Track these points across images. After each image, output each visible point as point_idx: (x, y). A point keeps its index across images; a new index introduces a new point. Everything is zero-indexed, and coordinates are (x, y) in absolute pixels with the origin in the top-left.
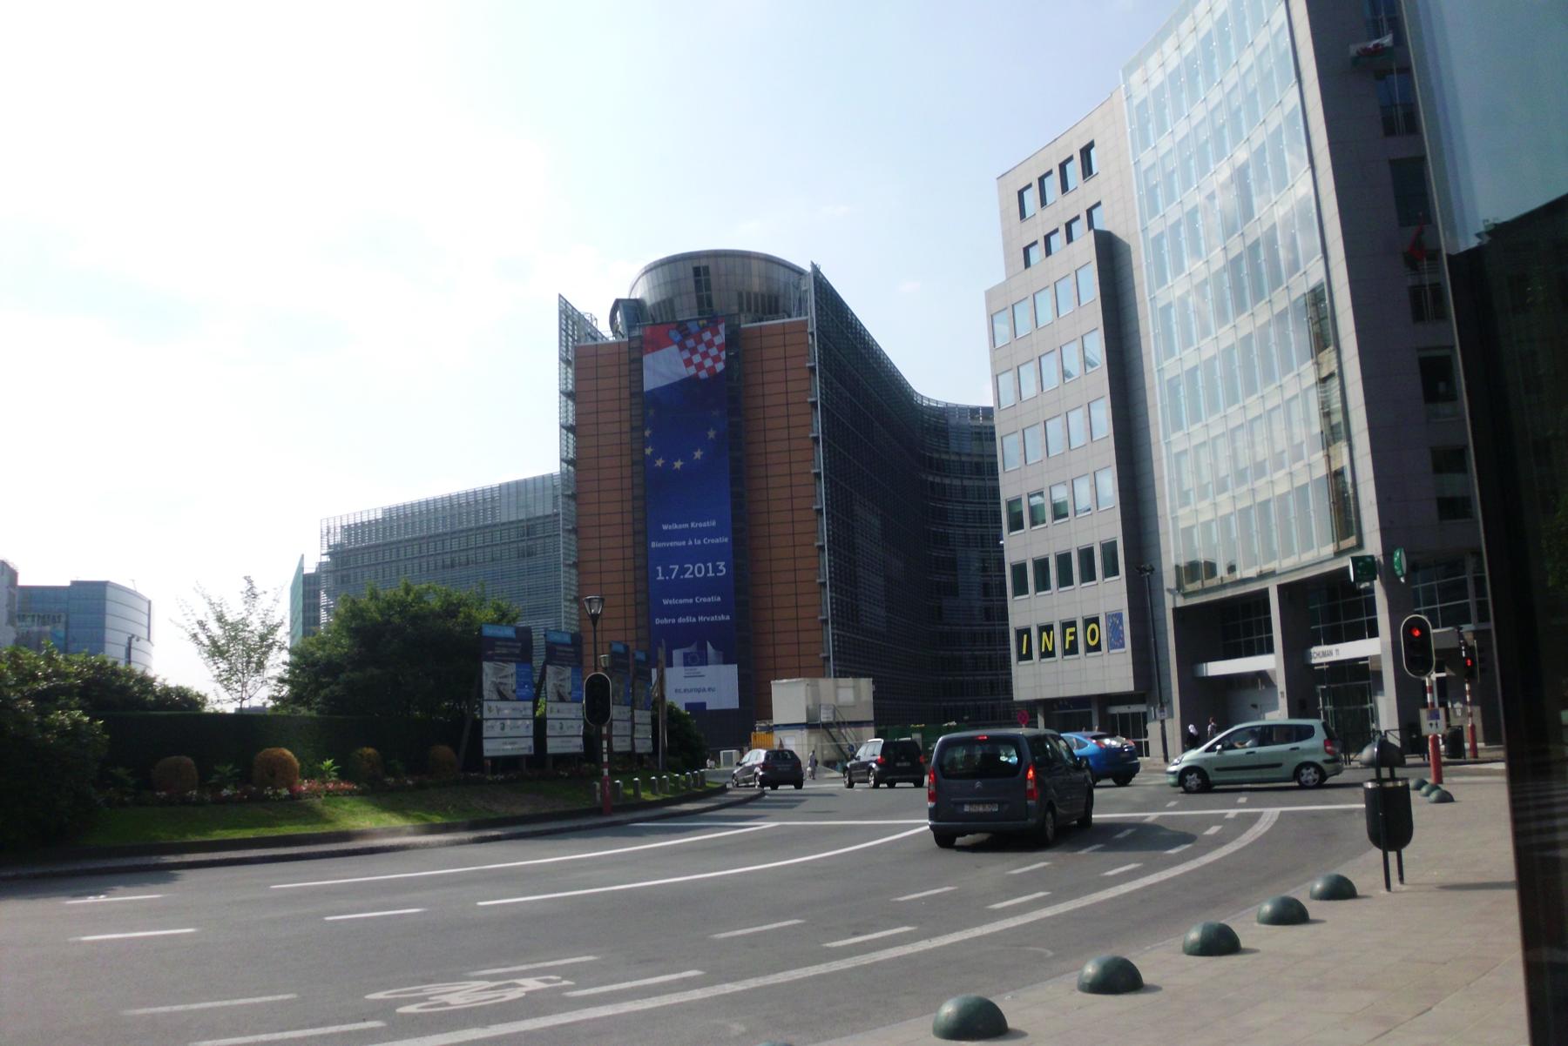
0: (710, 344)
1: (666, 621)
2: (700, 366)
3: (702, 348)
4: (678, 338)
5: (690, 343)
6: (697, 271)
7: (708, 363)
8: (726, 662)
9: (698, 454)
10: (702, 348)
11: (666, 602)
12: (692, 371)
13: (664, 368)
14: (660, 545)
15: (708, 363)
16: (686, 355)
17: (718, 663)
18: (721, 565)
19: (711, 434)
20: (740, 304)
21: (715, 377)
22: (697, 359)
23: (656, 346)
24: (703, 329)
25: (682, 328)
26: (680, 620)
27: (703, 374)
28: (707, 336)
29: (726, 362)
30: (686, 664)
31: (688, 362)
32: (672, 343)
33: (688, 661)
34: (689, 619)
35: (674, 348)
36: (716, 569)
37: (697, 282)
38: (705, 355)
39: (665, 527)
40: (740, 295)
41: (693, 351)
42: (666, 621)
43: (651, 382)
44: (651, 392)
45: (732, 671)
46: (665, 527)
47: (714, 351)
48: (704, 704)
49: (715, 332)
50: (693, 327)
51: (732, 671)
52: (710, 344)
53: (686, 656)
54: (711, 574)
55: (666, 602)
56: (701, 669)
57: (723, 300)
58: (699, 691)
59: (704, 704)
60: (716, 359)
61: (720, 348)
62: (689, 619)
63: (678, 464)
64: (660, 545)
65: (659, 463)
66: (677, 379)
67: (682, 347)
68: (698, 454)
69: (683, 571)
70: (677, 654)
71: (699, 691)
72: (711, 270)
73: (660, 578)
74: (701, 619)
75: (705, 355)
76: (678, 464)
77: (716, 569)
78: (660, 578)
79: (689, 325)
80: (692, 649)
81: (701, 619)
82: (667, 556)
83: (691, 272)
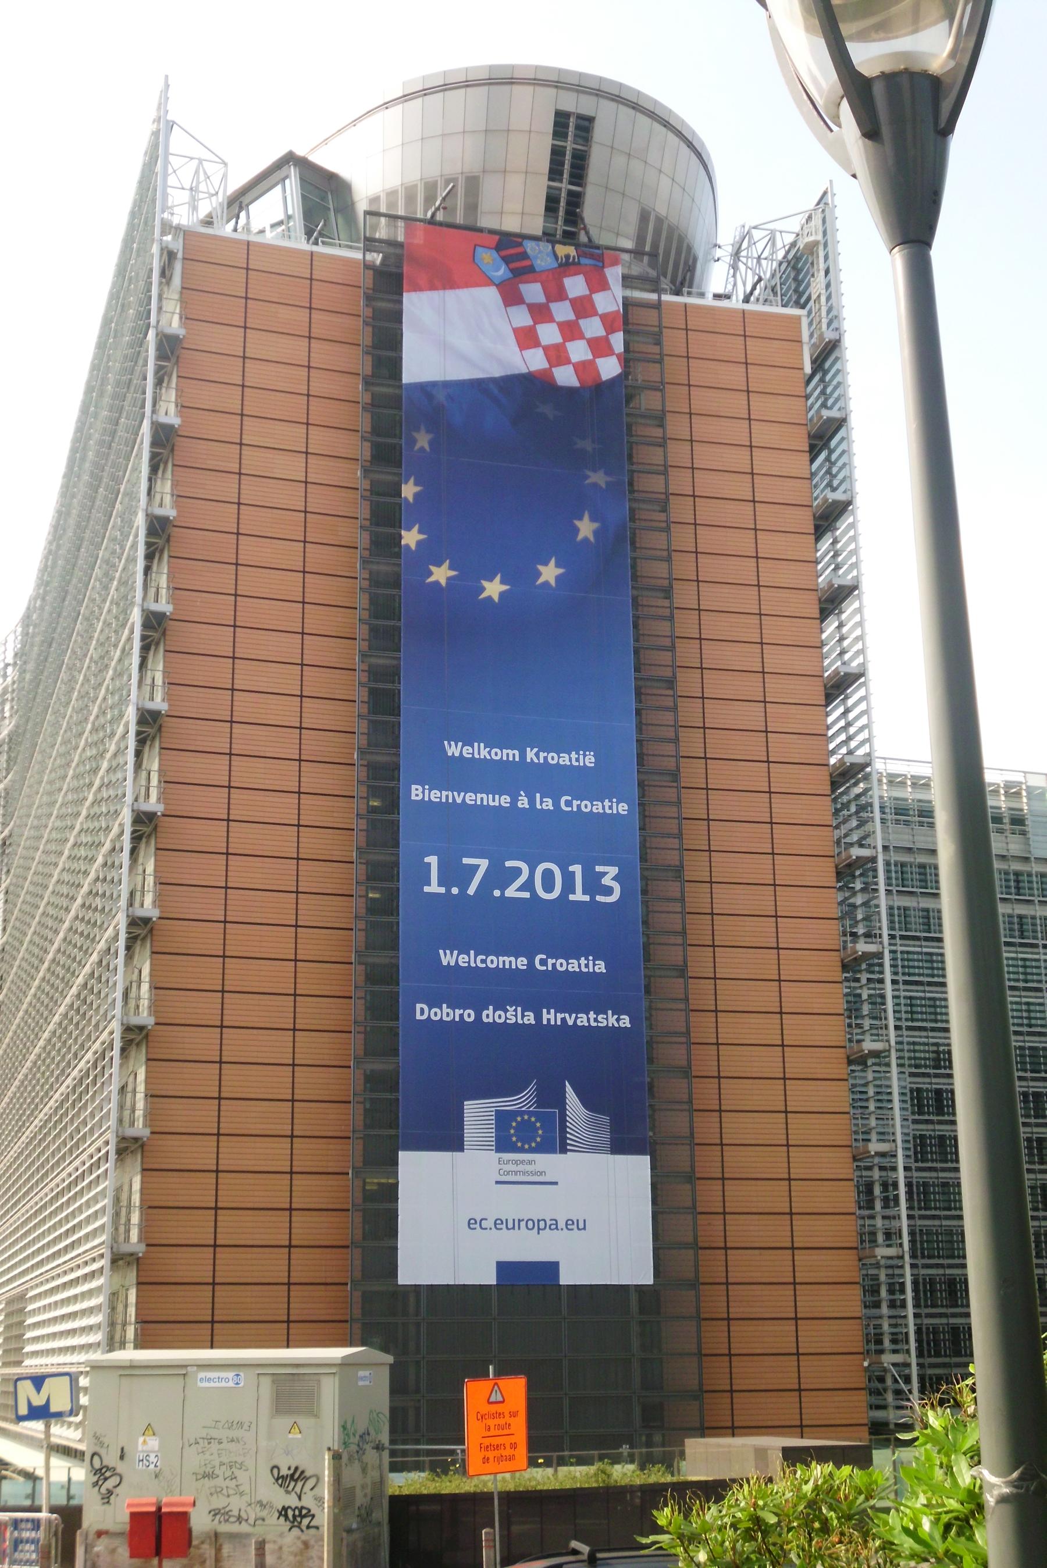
0: (583, 308)
1: (445, 1013)
2: (557, 355)
3: (562, 311)
4: (501, 272)
5: (533, 292)
6: (561, 120)
7: (579, 351)
8: (618, 1147)
9: (549, 573)
10: (562, 311)
11: (447, 958)
12: (535, 361)
13: (456, 338)
14: (435, 796)
15: (579, 351)
16: (522, 317)
17: (595, 1149)
18: (609, 874)
19: (586, 528)
20: (641, 239)
21: (596, 391)
22: (549, 334)
23: (444, 279)
24: (567, 266)
25: (508, 244)
26: (490, 1015)
27: (565, 377)
28: (576, 286)
29: (627, 360)
30: (503, 1145)
31: (527, 338)
32: (488, 282)
33: (509, 1137)
34: (513, 1015)
35: (490, 295)
36: (593, 884)
37: (557, 154)
38: (571, 331)
39: (453, 749)
40: (644, 217)
41: (540, 313)
42: (445, 1013)
43: (421, 363)
44: (425, 389)
45: (637, 1169)
46: (453, 749)
47: (593, 327)
48: (552, 1268)
49: (599, 284)
50: (542, 256)
51: (637, 1169)
52: (583, 308)
53: (503, 1119)
54: (579, 896)
55: (447, 958)
56: (546, 1162)
57: (608, 219)
58: (538, 1225)
59: (552, 1268)
60: (599, 347)
61: (609, 322)
62: (513, 1015)
63: (493, 589)
64: (435, 796)
65: (441, 574)
66: (497, 372)
67: (511, 297)
68: (549, 573)
69: (500, 877)
70: (478, 1115)
71: (538, 1225)
72: (600, 133)
73: (434, 887)
74: (550, 1017)
75: (571, 331)
76: (493, 589)
77: (593, 884)
78: (434, 887)
79: (530, 246)
80: (521, 1101)
81: (550, 1017)
82: (458, 830)
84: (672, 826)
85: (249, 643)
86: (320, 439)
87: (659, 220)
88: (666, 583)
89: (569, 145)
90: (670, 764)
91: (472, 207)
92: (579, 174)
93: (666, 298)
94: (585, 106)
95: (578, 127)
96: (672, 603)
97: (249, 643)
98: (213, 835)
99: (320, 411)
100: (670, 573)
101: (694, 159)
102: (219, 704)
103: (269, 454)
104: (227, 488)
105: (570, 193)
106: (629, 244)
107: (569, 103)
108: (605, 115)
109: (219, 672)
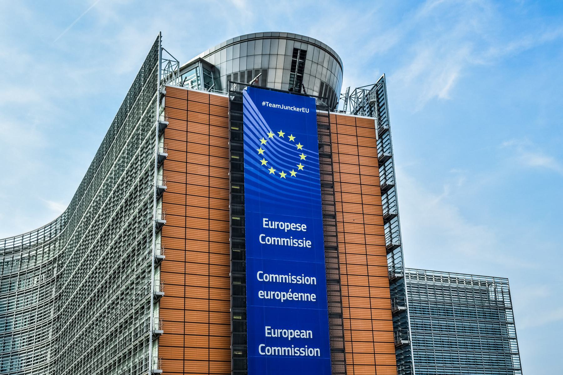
6: (295, 51)
20: (320, 93)
37: (294, 63)
40: (322, 84)
72: (309, 56)
83: (290, 53)
84: (338, 299)
85: (191, 234)
86: (213, 161)
87: (327, 86)
88: (333, 213)
89: (298, 60)
90: (337, 277)
91: (265, 80)
92: (301, 70)
93: (331, 113)
94: (303, 47)
95: (301, 54)
96: (336, 220)
97: (191, 234)
98: (179, 303)
99: (213, 151)
100: (335, 210)
101: (338, 65)
102: (180, 256)
103: (196, 166)
104: (182, 178)
105: (298, 76)
106: (316, 94)
107: (298, 45)
108: (310, 49)
109: (180, 244)
